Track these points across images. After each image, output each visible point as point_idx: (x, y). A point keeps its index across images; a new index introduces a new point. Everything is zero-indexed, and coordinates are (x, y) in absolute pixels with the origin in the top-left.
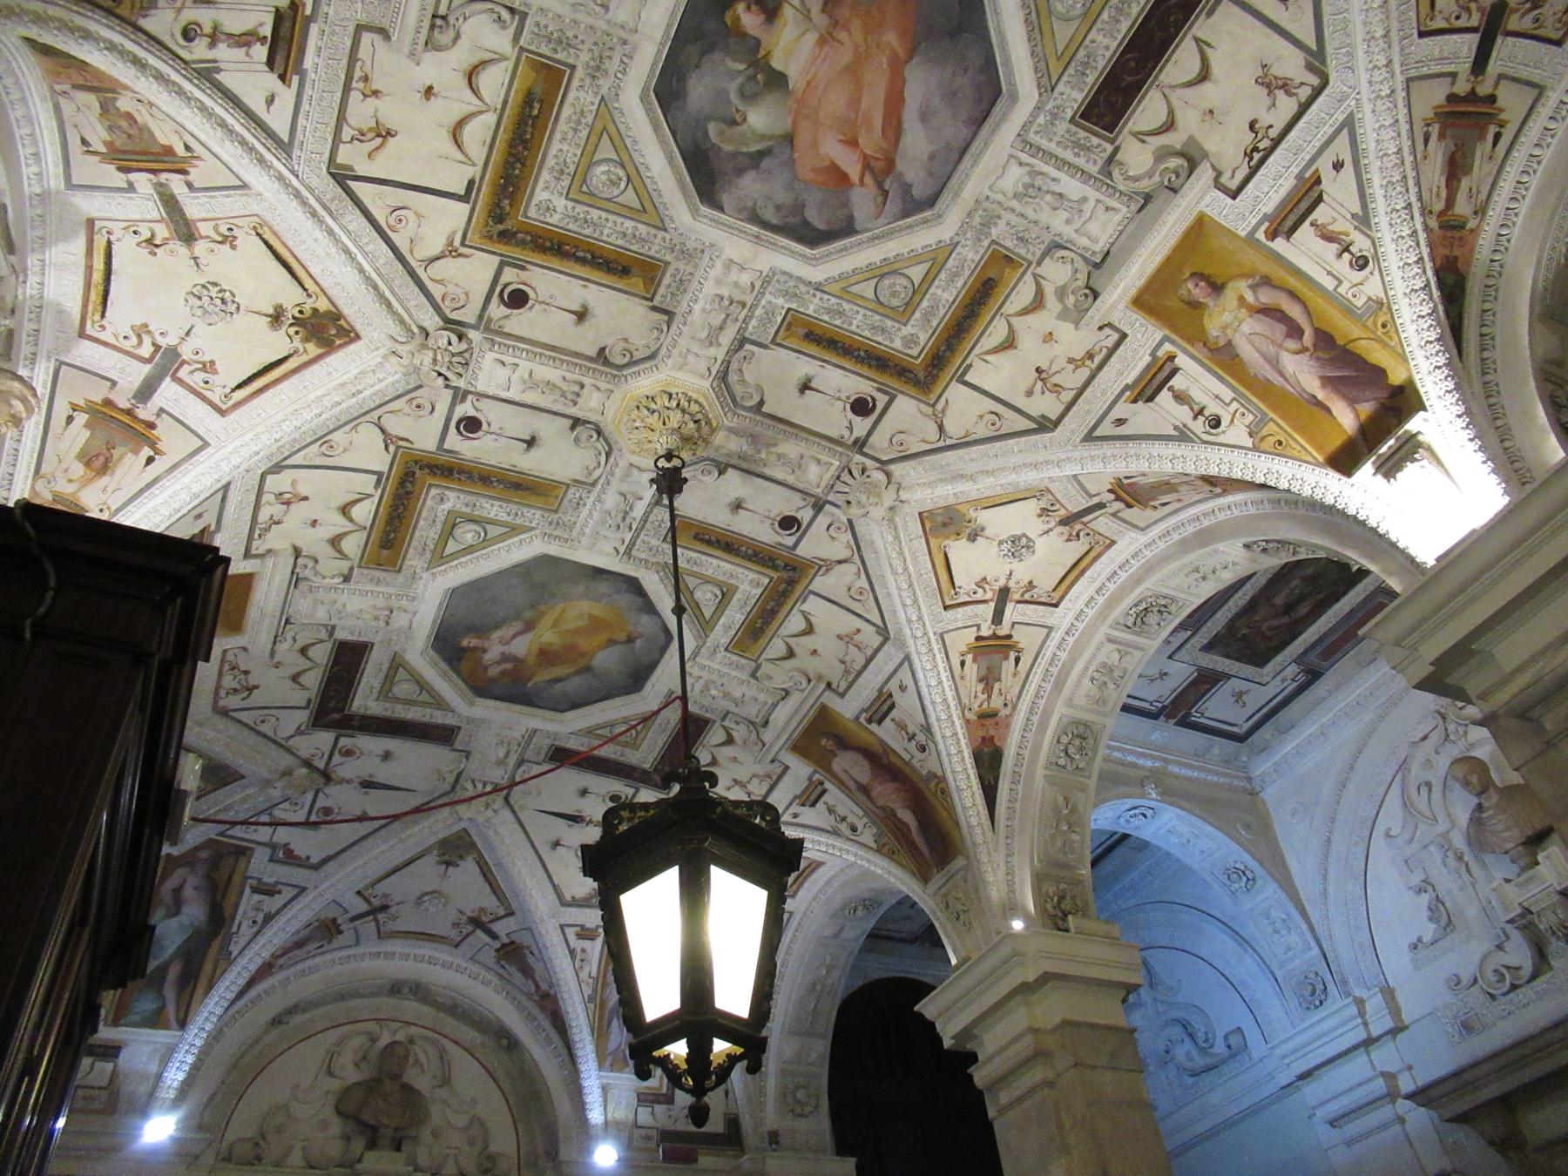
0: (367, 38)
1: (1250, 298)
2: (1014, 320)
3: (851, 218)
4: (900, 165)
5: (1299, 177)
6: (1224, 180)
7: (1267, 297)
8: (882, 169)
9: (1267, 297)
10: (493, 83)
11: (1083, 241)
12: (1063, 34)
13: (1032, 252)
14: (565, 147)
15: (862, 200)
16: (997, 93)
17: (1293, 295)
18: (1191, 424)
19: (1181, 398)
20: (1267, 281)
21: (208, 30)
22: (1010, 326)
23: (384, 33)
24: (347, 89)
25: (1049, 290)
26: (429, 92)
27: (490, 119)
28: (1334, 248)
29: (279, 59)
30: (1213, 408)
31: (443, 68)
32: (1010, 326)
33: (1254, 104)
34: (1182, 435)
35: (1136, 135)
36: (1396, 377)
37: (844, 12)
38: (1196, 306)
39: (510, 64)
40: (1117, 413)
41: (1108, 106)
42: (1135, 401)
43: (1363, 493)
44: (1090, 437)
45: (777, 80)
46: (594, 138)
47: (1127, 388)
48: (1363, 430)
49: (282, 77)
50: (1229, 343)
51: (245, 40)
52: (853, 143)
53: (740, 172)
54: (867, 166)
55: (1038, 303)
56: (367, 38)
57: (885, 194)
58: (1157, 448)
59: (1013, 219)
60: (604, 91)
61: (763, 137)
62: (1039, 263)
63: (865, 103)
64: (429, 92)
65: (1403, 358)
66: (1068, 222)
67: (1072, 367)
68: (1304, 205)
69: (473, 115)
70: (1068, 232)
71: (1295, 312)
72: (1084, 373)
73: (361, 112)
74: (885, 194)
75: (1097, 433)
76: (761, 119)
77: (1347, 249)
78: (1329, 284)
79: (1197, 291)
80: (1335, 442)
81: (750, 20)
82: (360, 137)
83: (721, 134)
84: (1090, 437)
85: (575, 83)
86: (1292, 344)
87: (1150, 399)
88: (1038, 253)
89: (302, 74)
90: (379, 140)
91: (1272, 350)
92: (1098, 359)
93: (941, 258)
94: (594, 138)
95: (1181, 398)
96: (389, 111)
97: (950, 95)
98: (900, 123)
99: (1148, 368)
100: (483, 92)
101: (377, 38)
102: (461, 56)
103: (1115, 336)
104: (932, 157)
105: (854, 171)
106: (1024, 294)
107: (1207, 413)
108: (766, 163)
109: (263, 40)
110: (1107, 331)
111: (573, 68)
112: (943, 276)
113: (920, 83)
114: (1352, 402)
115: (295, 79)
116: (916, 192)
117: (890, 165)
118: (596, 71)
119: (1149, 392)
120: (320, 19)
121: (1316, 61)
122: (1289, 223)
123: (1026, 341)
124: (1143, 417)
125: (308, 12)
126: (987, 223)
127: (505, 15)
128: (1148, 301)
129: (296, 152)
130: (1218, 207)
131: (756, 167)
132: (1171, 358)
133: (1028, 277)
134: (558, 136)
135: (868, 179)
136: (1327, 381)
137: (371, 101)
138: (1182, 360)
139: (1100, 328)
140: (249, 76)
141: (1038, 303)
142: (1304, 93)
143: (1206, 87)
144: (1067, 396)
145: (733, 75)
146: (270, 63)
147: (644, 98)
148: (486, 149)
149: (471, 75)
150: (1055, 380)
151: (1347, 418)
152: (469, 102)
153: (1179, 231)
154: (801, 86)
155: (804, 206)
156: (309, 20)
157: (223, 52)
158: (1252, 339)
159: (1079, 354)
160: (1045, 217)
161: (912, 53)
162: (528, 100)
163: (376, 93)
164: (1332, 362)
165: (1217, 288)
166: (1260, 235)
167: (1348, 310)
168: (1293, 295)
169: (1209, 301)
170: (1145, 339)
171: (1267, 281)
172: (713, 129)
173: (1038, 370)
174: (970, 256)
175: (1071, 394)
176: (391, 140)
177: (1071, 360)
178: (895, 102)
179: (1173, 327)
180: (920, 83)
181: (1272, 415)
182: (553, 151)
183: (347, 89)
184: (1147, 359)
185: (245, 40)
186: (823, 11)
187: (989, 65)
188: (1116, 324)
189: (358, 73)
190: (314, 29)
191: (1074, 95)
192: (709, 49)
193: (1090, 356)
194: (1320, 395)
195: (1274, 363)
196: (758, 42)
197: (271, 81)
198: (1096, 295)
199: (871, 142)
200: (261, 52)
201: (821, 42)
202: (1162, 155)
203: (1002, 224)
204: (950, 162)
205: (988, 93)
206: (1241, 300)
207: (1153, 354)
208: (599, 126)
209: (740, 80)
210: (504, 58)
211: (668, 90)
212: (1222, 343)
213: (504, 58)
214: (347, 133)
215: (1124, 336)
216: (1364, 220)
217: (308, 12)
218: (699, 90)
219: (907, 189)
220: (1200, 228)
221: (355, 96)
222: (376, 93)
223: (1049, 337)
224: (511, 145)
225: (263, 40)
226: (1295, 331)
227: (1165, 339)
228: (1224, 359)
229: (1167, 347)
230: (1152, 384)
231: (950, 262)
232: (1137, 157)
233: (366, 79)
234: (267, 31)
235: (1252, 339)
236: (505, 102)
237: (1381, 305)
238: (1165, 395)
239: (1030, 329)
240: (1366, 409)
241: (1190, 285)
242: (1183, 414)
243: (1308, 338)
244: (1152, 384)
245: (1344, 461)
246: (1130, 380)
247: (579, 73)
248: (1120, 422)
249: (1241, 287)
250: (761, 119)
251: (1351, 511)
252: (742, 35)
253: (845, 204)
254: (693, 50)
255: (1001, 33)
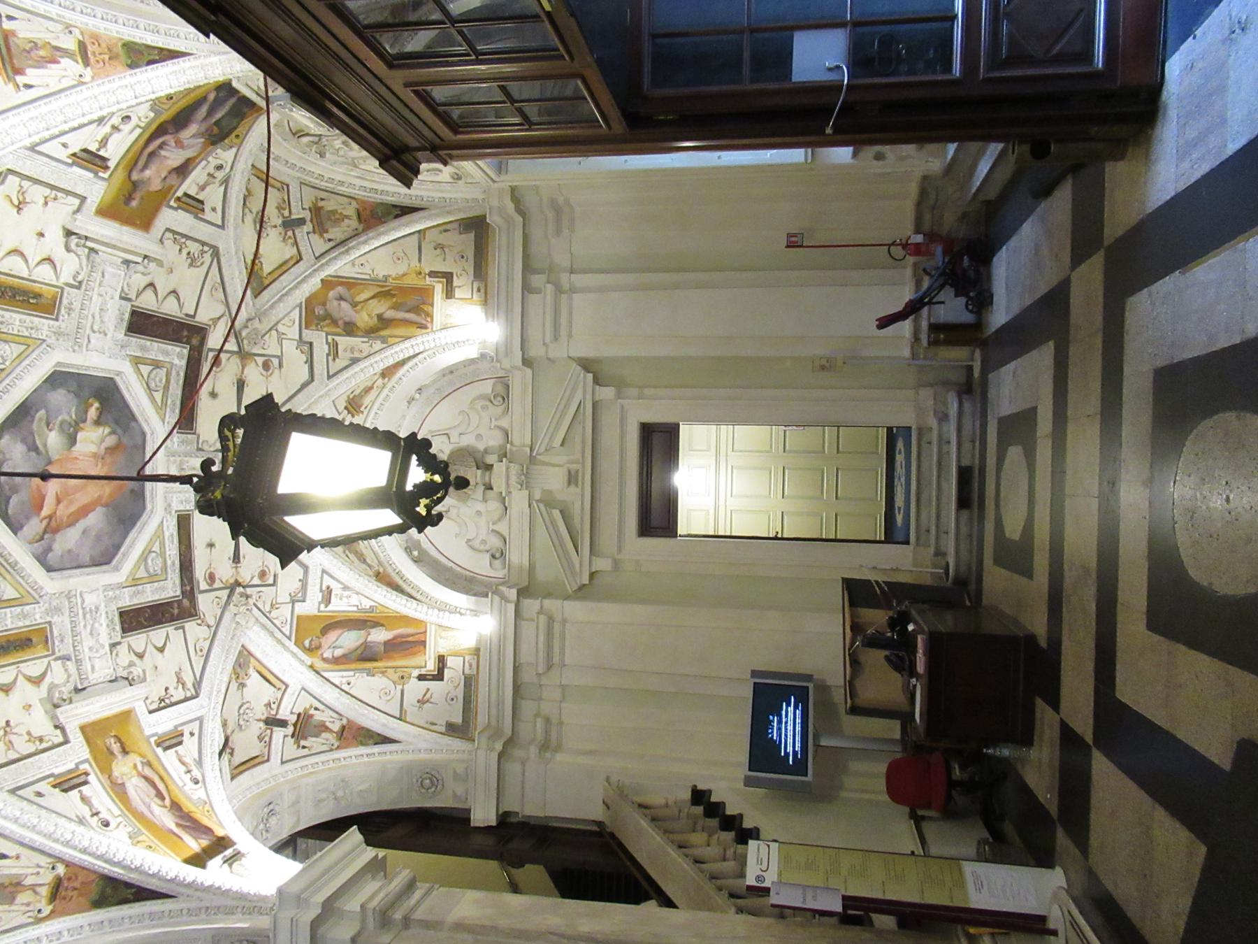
0: (77, 202)
1: (140, 767)
2: (20, 677)
3: (21, 527)
4: (58, 536)
5: (176, 727)
6: (148, 702)
7: (148, 772)
8: (53, 528)
9: (148, 772)
10: (44, 274)
11: (87, 666)
12: (141, 573)
13: (62, 648)
14: (17, 323)
15: (34, 526)
16: (108, 563)
17: (162, 778)
18: (88, 817)
19: (84, 799)
20: (149, 764)
21: (121, 127)
22: (16, 679)
23: (78, 210)
24: (53, 187)
25: (48, 680)
26: (41, 235)
27: (25, 274)
28: (184, 769)
29: (85, 155)
30: (104, 815)
31: (54, 243)
32: (16, 679)
33: (172, 683)
34: (81, 821)
35: (129, 646)
36: (220, 832)
37: (108, 459)
38: (112, 753)
39: (54, 283)
40: (37, 787)
41: (135, 620)
42: (55, 786)
43: (215, 873)
44: (13, 791)
45: (73, 440)
46: (22, 340)
47: (52, 775)
48: (204, 850)
49: (74, 155)
50: (123, 784)
51: (104, 143)
52: (59, 501)
53: (24, 441)
54: (50, 517)
55: (37, 681)
56: (77, 202)
57: (42, 538)
58: (62, 821)
59: (67, 622)
60: (49, 341)
61: (45, 445)
62: (56, 659)
63: (78, 495)
64: (41, 235)
65: (221, 824)
66: (91, 649)
67: (27, 738)
68: (174, 741)
69: (26, 261)
70: (86, 653)
71: (161, 786)
72: (31, 748)
73: (37, 194)
74: (42, 538)
75: (19, 793)
76: (54, 440)
77: (189, 772)
78: (181, 784)
79: (116, 748)
80: (188, 854)
81: (93, 413)
82: (22, 192)
83: (40, 419)
84: (13, 791)
85: (52, 322)
86: (156, 800)
87: (65, 791)
88: (61, 654)
89: (71, 165)
90: (16, 203)
91: (147, 800)
92: (44, 745)
93: (25, 601)
94: (22, 340)
95: (84, 799)
96: (34, 211)
97: (98, 538)
98: (77, 521)
99: (70, 771)
100: (40, 267)
101: (75, 207)
102: (59, 253)
103: (61, 739)
104: (69, 551)
105: (45, 512)
106: (34, 669)
107: (101, 816)
108: (33, 454)
109: (98, 150)
110: (58, 732)
111: (57, 320)
112: (19, 609)
113: (95, 519)
114: (196, 838)
115: (70, 161)
116: (50, 555)
117: (56, 531)
118: (58, 334)
119: (66, 786)
120: (95, 180)
121: (198, 685)
122: (167, 743)
123: (16, 696)
124: (56, 798)
125: (101, 174)
126: (58, 610)
127: (80, 278)
128: (89, 731)
129: (28, 153)
130: (141, 710)
131: (29, 450)
132: (87, 774)
133: (46, 660)
134: (24, 317)
135: (45, 522)
136: (178, 825)
137: (42, 201)
138: (92, 778)
139: (56, 727)
140: (87, 139)
141: (37, 681)
142: (189, 695)
143: (160, 655)
144: (14, 756)
145: (69, 413)
146: (85, 151)
147: (59, 364)
148: (7, 271)
149: (48, 260)
150: (13, 738)
151: (194, 845)
152: (33, 258)
153: (116, 710)
154: (75, 454)
155: (17, 492)
156: (96, 174)
157: (107, 129)
158: (136, 788)
159: (36, 734)
160: (85, 634)
161: (106, 505)
162: (38, 296)
163: (46, 203)
164: (181, 817)
165: (125, 752)
166: (152, 740)
167: (189, 799)
168: (162, 778)
169: (120, 757)
170: (77, 753)
171: (149, 764)
172: (42, 413)
173: (8, 722)
174: (36, 615)
175: (17, 756)
176: (15, 210)
177: (29, 733)
178: (84, 511)
179: (95, 759)
180: (95, 519)
181: (144, 831)
182: (14, 315)
183: (53, 187)
184: (72, 766)
185: (104, 143)
186: (107, 449)
187: (117, 547)
188: (68, 731)
189: (59, 195)
190: (91, 175)
191: (129, 600)
192: (77, 395)
193: (41, 740)
194: (176, 830)
195: (149, 807)
196: (85, 421)
197: (76, 149)
198: (71, 702)
199: (63, 511)
200: (93, 147)
201: (95, 455)
202: (131, 664)
203: (60, 619)
204: (73, 563)
205: (105, 558)
206: (135, 766)
207: (77, 765)
208: (29, 341)
209: (67, 418)
210: (58, 278)
211: (57, 379)
212: (120, 781)
213: (58, 278)
214: (26, 184)
215: (66, 742)
216: (200, 762)
217: (101, 174)
218: (59, 398)
219: (49, 549)
220: (126, 717)
221: (47, 191)
222: (46, 203)
223: (28, 707)
224: (12, 288)
225: (98, 150)
226: (160, 795)
227: (86, 761)
228: (118, 790)
229: (85, 766)
230: (69, 783)
231: (27, 607)
232: (124, 656)
233: (55, 199)
234: (102, 153)
235: (136, 788)
236: (34, 281)
237: (208, 802)
238: (75, 793)
239: (23, 691)
240: (205, 843)
241: (112, 740)
242: (85, 811)
243: (167, 802)
244: (69, 783)
245: (198, 860)
246: (56, 771)
247: (57, 324)
248: (39, 794)
249: (134, 758)
250: (54, 440)
251: (207, 884)
252: (86, 412)
253: (28, 518)
254: (74, 387)
255: (133, 543)
